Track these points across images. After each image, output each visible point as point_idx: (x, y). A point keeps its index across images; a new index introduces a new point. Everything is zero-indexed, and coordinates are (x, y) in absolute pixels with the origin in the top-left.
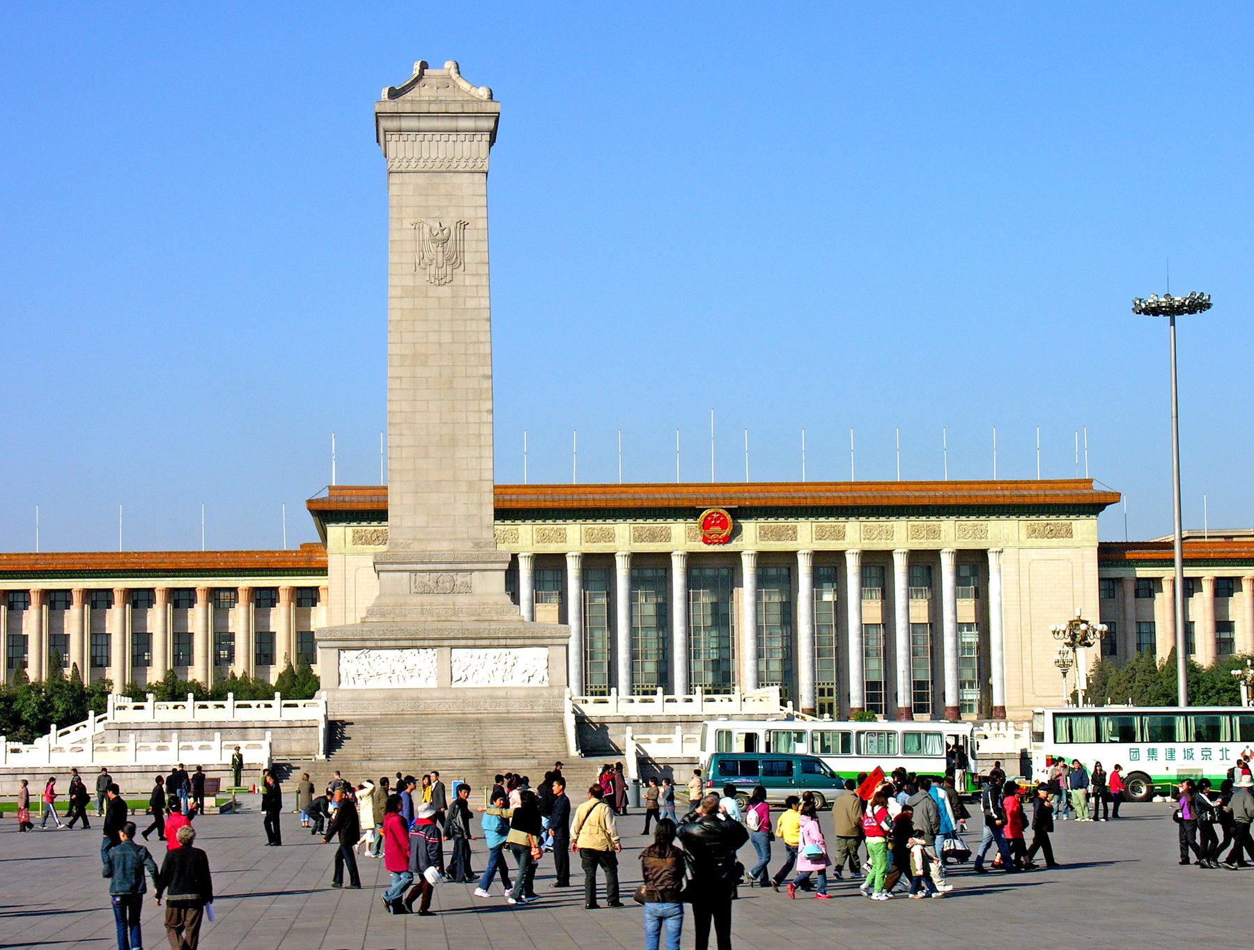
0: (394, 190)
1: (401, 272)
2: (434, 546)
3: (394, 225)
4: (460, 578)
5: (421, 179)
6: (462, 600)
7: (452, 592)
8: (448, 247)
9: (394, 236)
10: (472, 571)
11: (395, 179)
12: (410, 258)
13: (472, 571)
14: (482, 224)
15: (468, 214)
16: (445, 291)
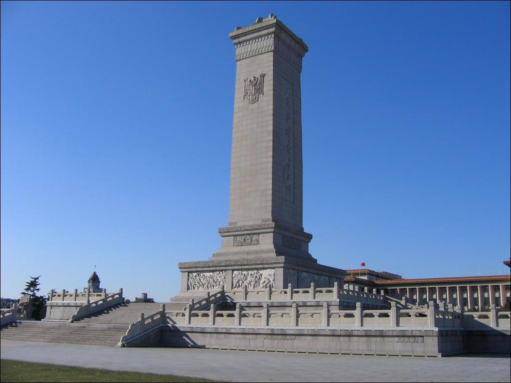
0: (238, 68)
1: (239, 101)
2: (246, 223)
3: (237, 82)
4: (255, 237)
5: (248, 60)
6: (253, 248)
7: (251, 244)
8: (257, 85)
9: (237, 86)
10: (259, 234)
11: (238, 63)
12: (243, 94)
13: (259, 234)
14: (272, 73)
15: (265, 71)
16: (255, 105)
